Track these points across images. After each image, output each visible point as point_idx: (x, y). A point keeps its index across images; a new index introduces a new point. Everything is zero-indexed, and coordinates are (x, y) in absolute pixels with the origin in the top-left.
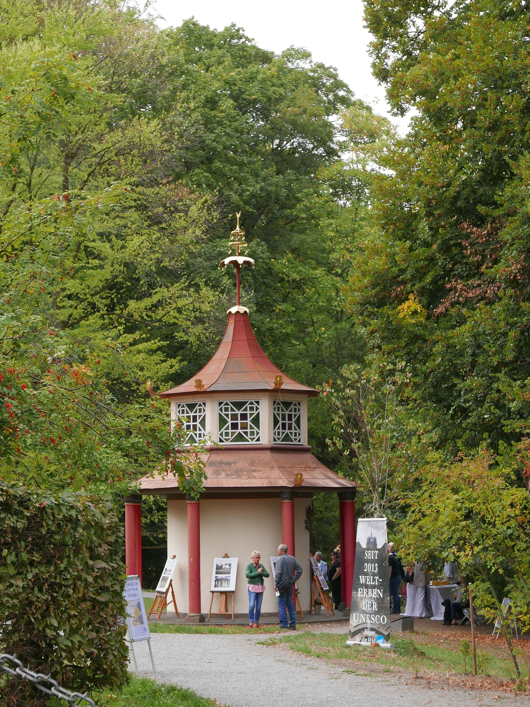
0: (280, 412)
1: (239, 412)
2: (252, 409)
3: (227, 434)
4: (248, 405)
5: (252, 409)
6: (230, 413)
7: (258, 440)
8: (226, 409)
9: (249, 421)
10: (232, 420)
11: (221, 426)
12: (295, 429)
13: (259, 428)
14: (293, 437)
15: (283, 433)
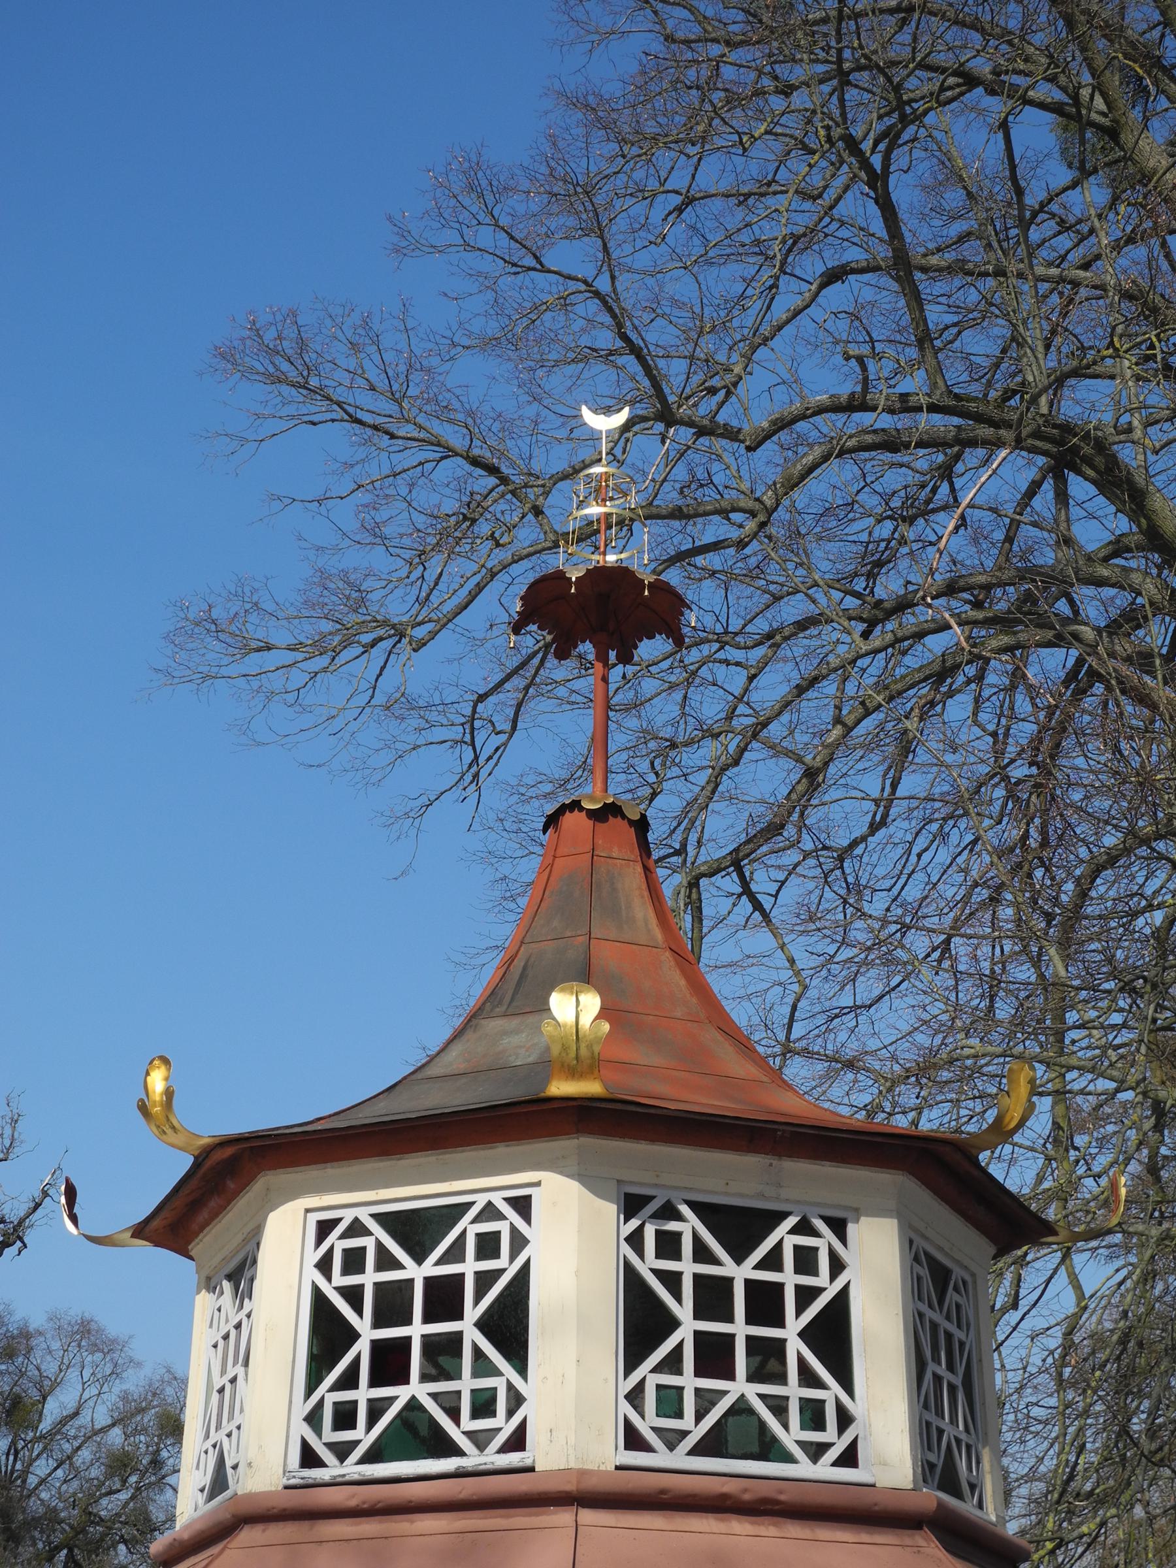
0: (687, 1267)
1: (416, 1272)
2: (488, 1246)
3: (345, 1417)
4: (469, 1227)
5: (488, 1246)
6: (369, 1278)
7: (517, 1441)
8: (354, 1259)
9: (467, 1327)
10: (377, 1324)
11: (319, 1363)
12: (808, 1378)
13: (523, 1371)
14: (791, 1436)
15: (706, 1400)
